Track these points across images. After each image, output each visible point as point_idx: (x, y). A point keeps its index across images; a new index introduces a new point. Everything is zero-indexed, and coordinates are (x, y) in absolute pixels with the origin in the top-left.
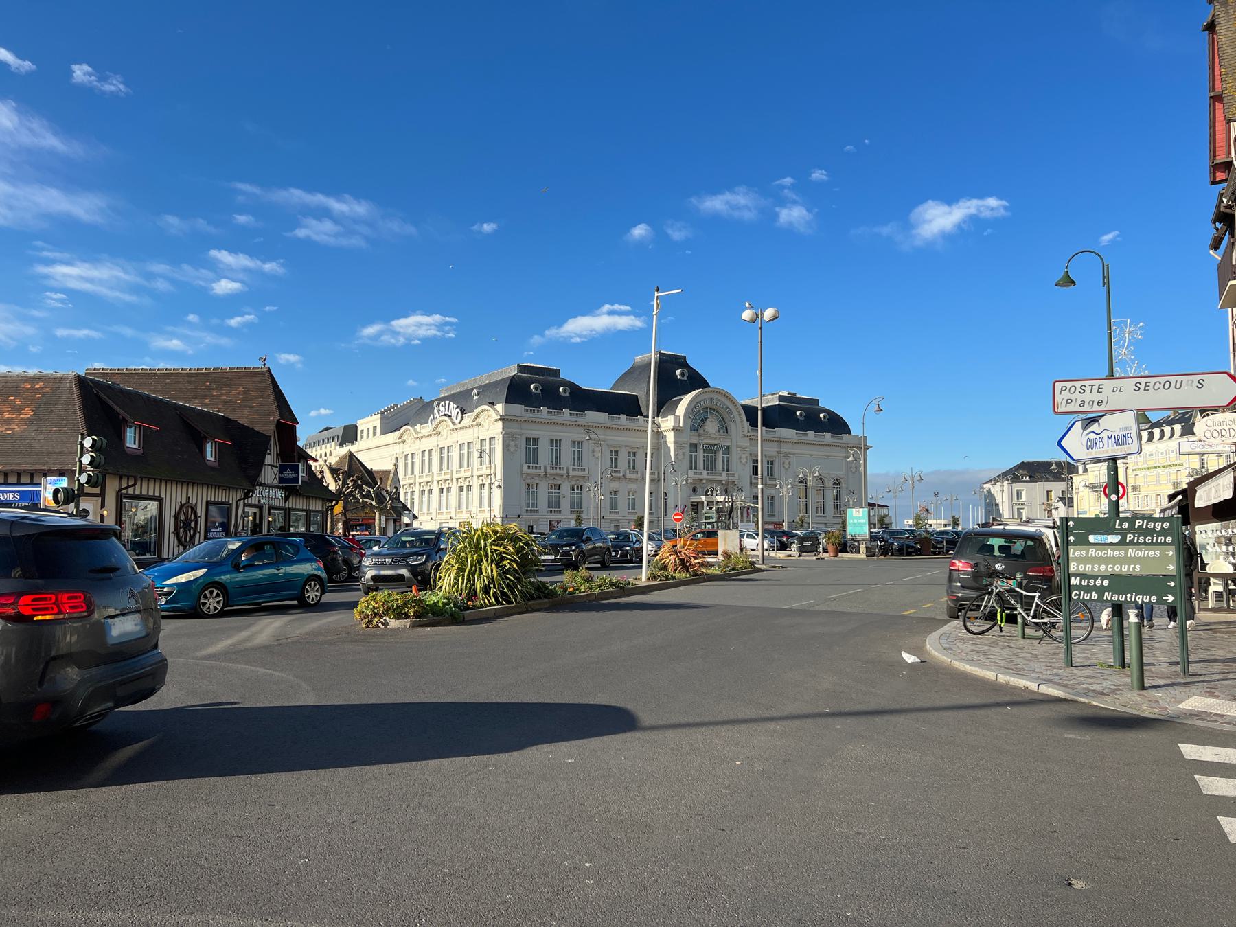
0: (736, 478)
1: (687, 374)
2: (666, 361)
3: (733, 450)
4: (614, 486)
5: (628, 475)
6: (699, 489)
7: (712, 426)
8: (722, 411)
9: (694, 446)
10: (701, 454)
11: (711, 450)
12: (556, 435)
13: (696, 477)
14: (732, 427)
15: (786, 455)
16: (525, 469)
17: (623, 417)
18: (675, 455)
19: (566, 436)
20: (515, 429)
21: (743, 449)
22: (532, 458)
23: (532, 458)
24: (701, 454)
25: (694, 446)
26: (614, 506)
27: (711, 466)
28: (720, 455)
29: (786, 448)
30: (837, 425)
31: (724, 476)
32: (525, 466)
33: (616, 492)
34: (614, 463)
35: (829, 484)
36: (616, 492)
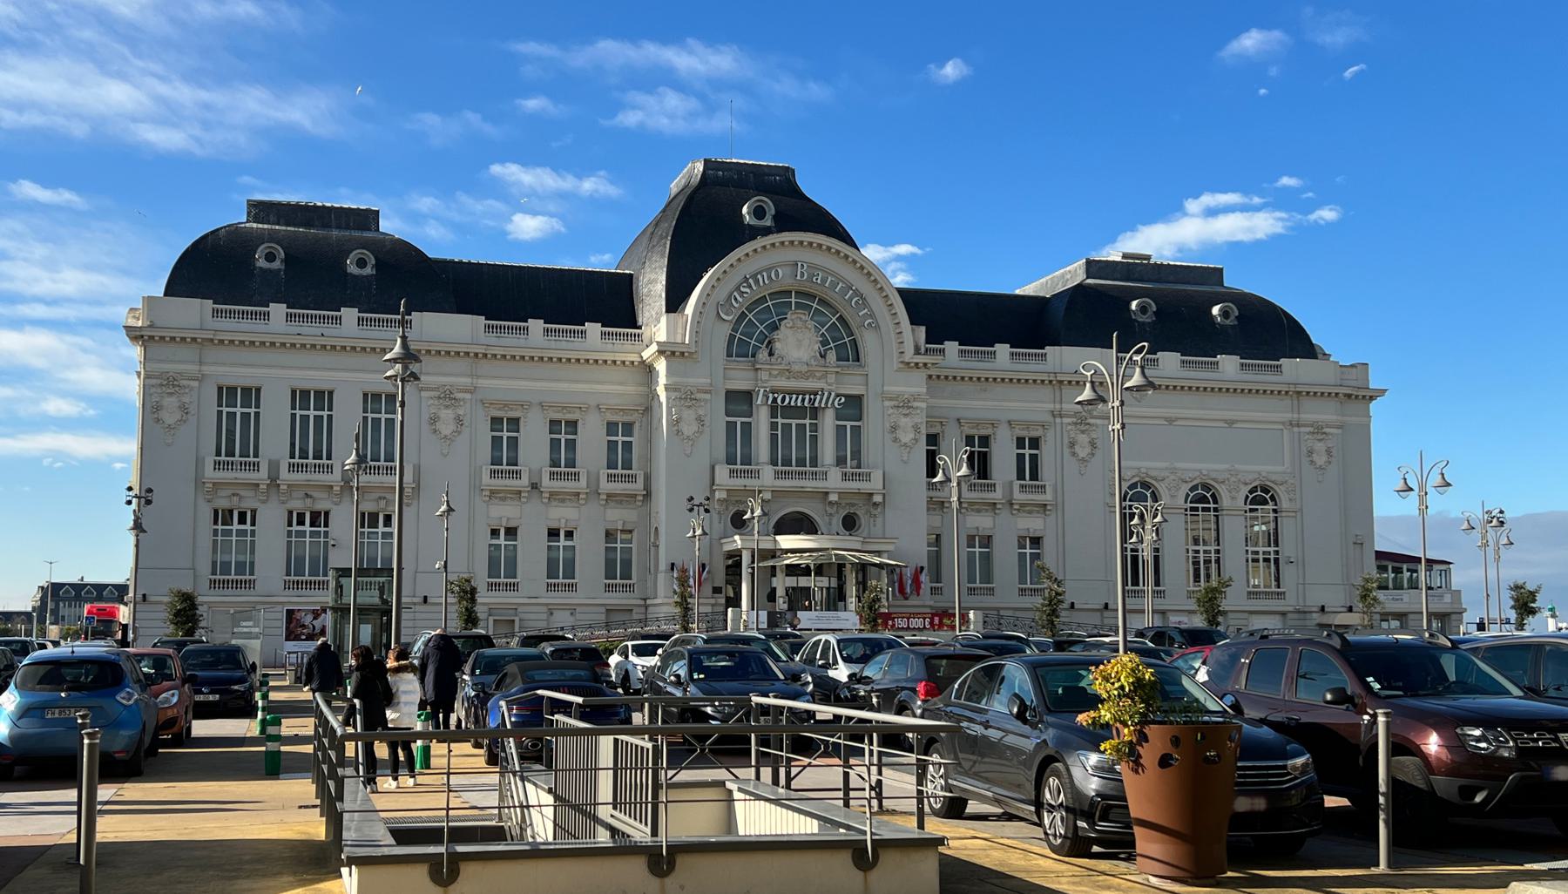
0: (875, 484)
1: (771, 209)
2: (723, 183)
3: (872, 409)
4: (504, 513)
5: (546, 482)
7: (797, 342)
8: (832, 297)
9: (739, 401)
10: (762, 420)
11: (796, 412)
12: (313, 377)
13: (739, 483)
14: (869, 343)
16: (210, 473)
17: (536, 325)
18: (675, 424)
20: (181, 362)
21: (905, 405)
22: (236, 441)
23: (236, 441)
24: (762, 420)
25: (739, 401)
27: (794, 454)
28: (828, 422)
30: (1269, 333)
31: (834, 481)
32: (210, 461)
33: (511, 532)
34: (504, 454)
36: (511, 532)
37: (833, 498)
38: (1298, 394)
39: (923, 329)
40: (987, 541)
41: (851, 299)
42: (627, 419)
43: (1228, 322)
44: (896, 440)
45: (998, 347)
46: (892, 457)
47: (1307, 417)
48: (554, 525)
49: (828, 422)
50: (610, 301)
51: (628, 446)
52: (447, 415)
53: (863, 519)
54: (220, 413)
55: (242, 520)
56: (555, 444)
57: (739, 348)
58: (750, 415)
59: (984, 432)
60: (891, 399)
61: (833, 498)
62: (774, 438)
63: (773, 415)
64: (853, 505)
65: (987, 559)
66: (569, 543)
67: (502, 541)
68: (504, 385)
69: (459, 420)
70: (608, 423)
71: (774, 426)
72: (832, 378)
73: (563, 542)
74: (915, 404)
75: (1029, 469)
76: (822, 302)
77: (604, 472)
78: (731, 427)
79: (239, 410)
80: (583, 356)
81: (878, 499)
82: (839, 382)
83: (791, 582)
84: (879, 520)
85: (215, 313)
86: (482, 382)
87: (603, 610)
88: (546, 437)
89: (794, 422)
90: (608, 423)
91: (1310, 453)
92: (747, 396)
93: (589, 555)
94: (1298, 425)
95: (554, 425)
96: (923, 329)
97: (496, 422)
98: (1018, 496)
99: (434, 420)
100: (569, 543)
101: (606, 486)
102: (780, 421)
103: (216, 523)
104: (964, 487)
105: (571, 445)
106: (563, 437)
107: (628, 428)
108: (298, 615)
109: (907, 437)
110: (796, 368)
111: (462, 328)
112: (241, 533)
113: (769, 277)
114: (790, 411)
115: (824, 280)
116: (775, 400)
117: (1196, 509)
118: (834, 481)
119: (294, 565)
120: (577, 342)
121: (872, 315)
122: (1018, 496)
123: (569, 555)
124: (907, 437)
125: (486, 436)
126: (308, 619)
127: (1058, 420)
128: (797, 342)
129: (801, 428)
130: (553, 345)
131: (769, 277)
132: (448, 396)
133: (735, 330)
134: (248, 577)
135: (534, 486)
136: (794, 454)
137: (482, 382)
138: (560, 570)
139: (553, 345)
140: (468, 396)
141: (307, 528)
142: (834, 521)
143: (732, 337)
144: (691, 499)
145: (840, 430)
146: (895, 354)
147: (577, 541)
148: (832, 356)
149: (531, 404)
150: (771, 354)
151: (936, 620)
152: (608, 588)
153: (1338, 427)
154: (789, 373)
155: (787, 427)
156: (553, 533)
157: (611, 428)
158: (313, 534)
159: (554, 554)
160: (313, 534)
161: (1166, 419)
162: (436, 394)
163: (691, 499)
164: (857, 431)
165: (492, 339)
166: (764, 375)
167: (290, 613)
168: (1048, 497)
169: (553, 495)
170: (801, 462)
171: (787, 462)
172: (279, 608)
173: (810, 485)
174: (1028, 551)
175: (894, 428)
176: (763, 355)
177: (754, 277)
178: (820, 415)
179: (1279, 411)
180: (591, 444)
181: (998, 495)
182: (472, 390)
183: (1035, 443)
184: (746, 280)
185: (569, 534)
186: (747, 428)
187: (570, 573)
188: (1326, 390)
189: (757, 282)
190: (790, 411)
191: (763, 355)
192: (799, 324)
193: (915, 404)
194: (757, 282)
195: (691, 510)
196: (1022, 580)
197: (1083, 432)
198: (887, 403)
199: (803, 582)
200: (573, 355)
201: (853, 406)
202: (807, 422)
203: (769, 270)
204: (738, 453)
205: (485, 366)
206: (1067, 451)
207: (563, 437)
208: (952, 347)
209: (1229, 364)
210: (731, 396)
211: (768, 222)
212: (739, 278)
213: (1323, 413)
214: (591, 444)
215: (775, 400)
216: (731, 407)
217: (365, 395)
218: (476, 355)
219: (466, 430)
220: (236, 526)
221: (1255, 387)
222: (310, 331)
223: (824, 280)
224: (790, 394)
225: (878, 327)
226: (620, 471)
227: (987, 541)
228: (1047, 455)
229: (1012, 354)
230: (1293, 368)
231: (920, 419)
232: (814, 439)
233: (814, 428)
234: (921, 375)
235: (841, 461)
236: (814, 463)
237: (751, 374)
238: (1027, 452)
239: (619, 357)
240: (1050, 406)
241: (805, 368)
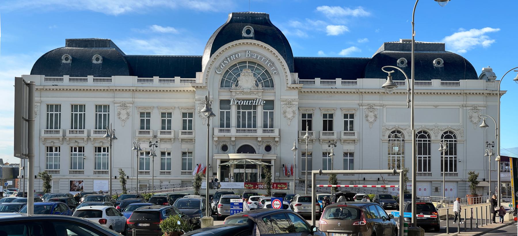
3: (277, 104)
6: (230, 148)
7: (247, 81)
8: (261, 62)
9: (225, 103)
10: (234, 111)
11: (247, 107)
12: (78, 101)
13: (222, 134)
15: (371, 107)
19: (90, 102)
21: (289, 103)
24: (234, 111)
25: (225, 103)
26: (143, 167)
27: (246, 122)
28: (260, 111)
29: (368, 100)
30: (457, 68)
34: (145, 125)
35: (436, 137)
37: (259, 139)
38: (466, 94)
39: (297, 74)
40: (352, 154)
43: (439, 66)
44: (285, 117)
46: (287, 122)
47: (470, 103)
48: (163, 151)
49: (260, 111)
50: (188, 67)
52: (124, 112)
54: (48, 114)
55: (104, 151)
56: (163, 122)
57: (225, 84)
58: (230, 109)
59: (331, 113)
60: (283, 101)
61: (259, 139)
62: (239, 117)
64: (268, 142)
67: (144, 156)
68: (145, 101)
69: (128, 114)
70: (183, 113)
71: (239, 113)
72: (260, 94)
73: (167, 156)
74: (293, 103)
76: (259, 65)
78: (222, 113)
79: (54, 113)
80: (172, 89)
81: (277, 139)
82: (261, 96)
83: (237, 171)
84: (278, 148)
85: (46, 79)
86: (136, 100)
89: (247, 111)
90: (183, 113)
91: (471, 117)
92: (229, 101)
93: (176, 160)
94: (466, 107)
95: (163, 114)
96: (297, 74)
97: (142, 114)
98: (322, 137)
99: (119, 114)
102: (241, 111)
103: (96, 152)
104: (321, 134)
106: (166, 119)
108: (74, 183)
109: (290, 116)
110: (245, 90)
111: (131, 81)
112: (56, 155)
113: (235, 57)
114: (245, 107)
115: (257, 57)
117: (447, 141)
118: (260, 132)
119: (73, 165)
120: (171, 84)
121: (276, 69)
122: (343, 137)
123: (169, 161)
124: (290, 116)
125: (138, 119)
126: (77, 184)
127: (361, 107)
128: (247, 81)
129: (250, 113)
130: (162, 85)
131: (235, 57)
132: (124, 106)
134: (106, 170)
136: (246, 122)
137: (136, 100)
138: (166, 167)
139: (162, 85)
140: (131, 105)
141: (77, 152)
142: (261, 148)
145: (265, 114)
146: (285, 84)
148: (260, 86)
149: (154, 107)
150: (236, 86)
151: (275, 185)
152: (183, 173)
153: (485, 107)
154: (242, 92)
155: (244, 113)
156: (184, 154)
157: (184, 115)
159: (163, 161)
161: (434, 106)
162: (119, 105)
164: (272, 114)
165: (140, 84)
166: (234, 94)
167: (71, 182)
168: (355, 137)
170: (249, 126)
171: (244, 126)
172: (67, 180)
173: (250, 134)
174: (348, 158)
175: (285, 112)
176: (234, 86)
177: (230, 57)
179: (458, 101)
180: (177, 121)
181: (335, 137)
182: (133, 103)
183: (352, 116)
184: (227, 58)
185: (169, 154)
186: (228, 113)
187: (169, 168)
188: (478, 92)
189: (231, 59)
190: (245, 107)
191: (234, 86)
192: (246, 74)
193: (293, 103)
194: (231, 59)
197: (371, 112)
198: (282, 103)
199: (242, 171)
200: (169, 89)
201: (269, 104)
202: (252, 111)
203: (235, 54)
204: (225, 124)
205: (137, 94)
206: (364, 119)
207: (166, 119)
209: (436, 83)
210: (222, 102)
211: (251, 35)
212: (224, 58)
213: (479, 101)
214: (177, 121)
216: (222, 106)
217: (96, 106)
218: (133, 90)
219: (130, 117)
220: (54, 152)
221: (449, 92)
222: (78, 84)
223: (257, 57)
224: (243, 100)
225: (278, 74)
227: (352, 154)
228: (356, 120)
229: (342, 82)
230: (465, 84)
231: (296, 108)
232: (255, 117)
233: (255, 113)
234: (296, 92)
236: (255, 126)
237: (229, 93)
238: (349, 120)
239: (186, 89)
240: (358, 102)
241: (249, 91)
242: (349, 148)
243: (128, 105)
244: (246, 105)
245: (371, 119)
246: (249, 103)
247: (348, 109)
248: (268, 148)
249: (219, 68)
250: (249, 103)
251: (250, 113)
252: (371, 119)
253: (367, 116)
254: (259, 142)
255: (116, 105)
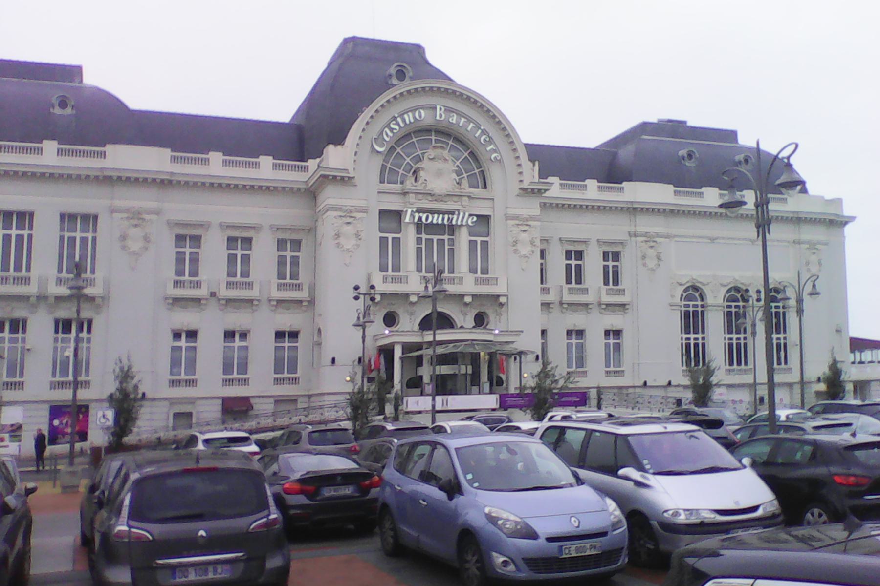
3: (496, 225)
4: (185, 319)
9: (391, 218)
14: (495, 175)
15: (650, 238)
21: (524, 222)
24: (409, 237)
25: (391, 218)
28: (463, 238)
33: (192, 335)
36: (192, 335)
37: (468, 299)
41: (480, 136)
42: (295, 236)
45: (588, 182)
51: (295, 261)
53: (492, 317)
62: (419, 251)
63: (419, 232)
65: (581, 348)
66: (243, 344)
71: (419, 240)
75: (612, 277)
77: (275, 281)
78: (383, 241)
87: (272, 400)
88: (223, 252)
89: (435, 238)
92: (398, 215)
97: (180, 239)
100: (243, 344)
101: (276, 294)
102: (424, 236)
105: (246, 259)
107: (297, 244)
109: (525, 250)
114: (433, 228)
116: (420, 219)
125: (169, 250)
127: (633, 239)
129: (441, 242)
132: (136, 217)
133: (386, 160)
135: (213, 294)
140: (154, 217)
143: (383, 168)
144: (356, 288)
145: (472, 244)
147: (250, 342)
155: (429, 242)
157: (281, 244)
158: (11, 340)
160: (11, 340)
162: (125, 215)
163: (356, 288)
169: (229, 301)
178: (456, 233)
184: (395, 118)
186: (397, 241)
195: (356, 298)
196: (607, 365)
202: (446, 237)
207: (239, 253)
208: (555, 180)
215: (420, 219)
216: (382, 225)
217: (62, 216)
226: (288, 280)
228: (626, 265)
232: (452, 251)
233: (452, 242)
235: (473, 270)
242: (614, 321)
243: (147, 217)
244: (437, 224)
245: (651, 263)
246: (443, 219)
247: (612, 243)
248: (480, 320)
249: (379, 139)
250: (443, 219)
251: (441, 242)
252: (651, 263)
253: (644, 257)
254: (466, 304)
255: (115, 215)
